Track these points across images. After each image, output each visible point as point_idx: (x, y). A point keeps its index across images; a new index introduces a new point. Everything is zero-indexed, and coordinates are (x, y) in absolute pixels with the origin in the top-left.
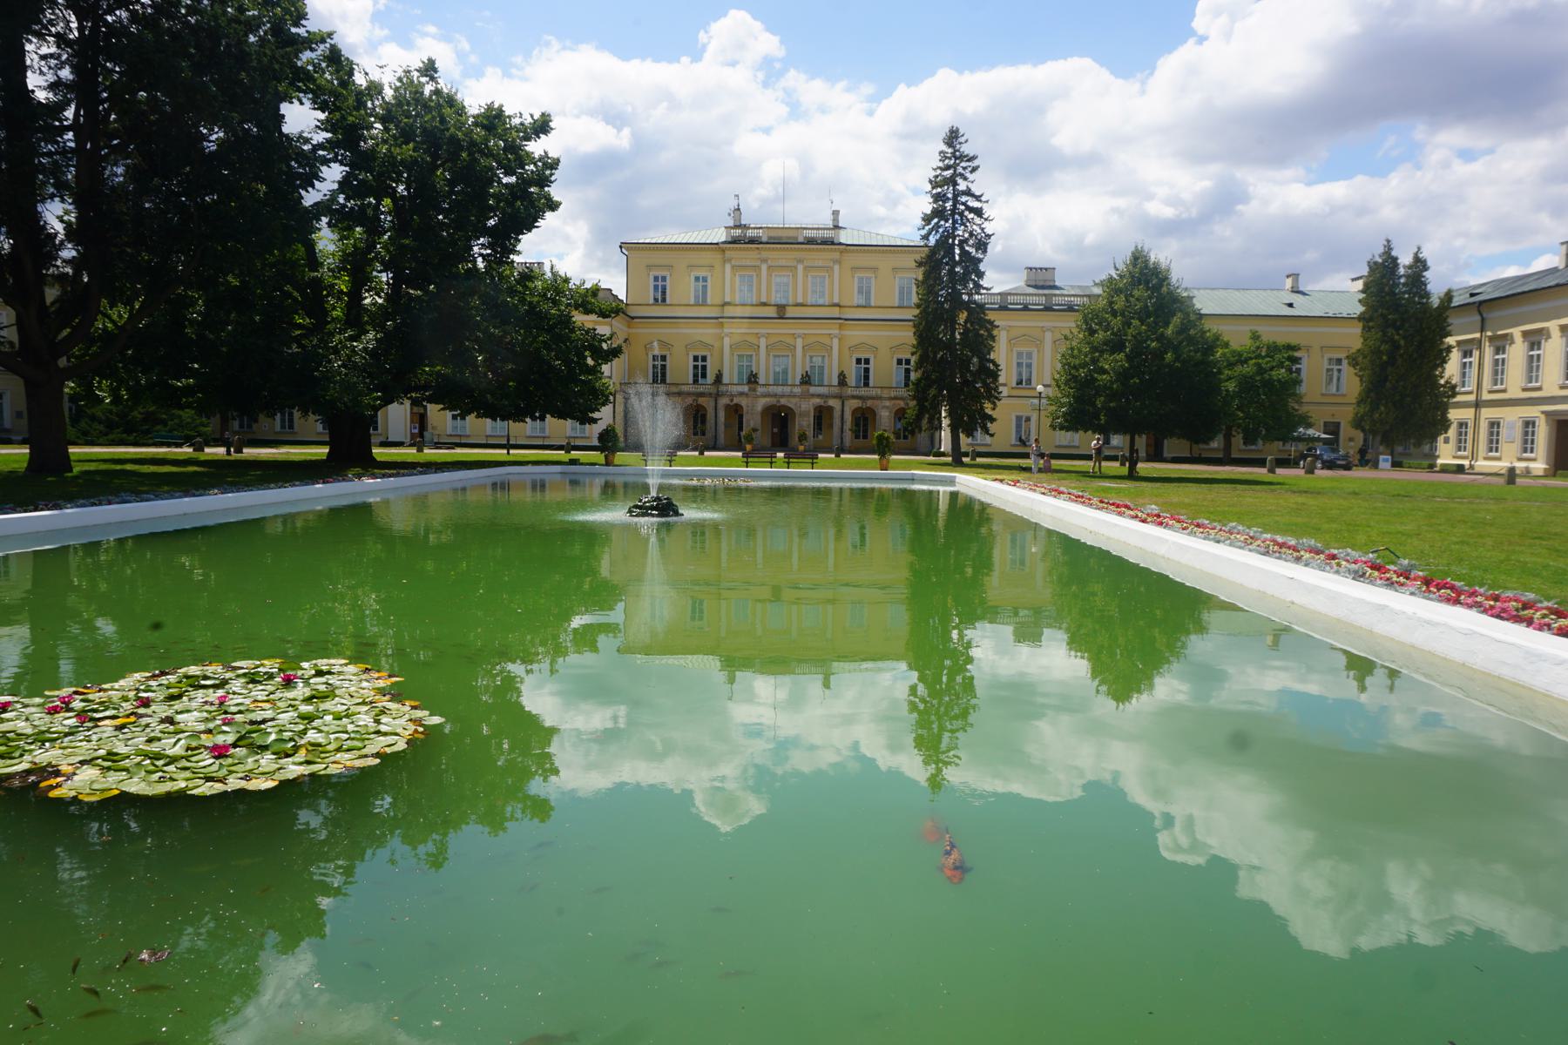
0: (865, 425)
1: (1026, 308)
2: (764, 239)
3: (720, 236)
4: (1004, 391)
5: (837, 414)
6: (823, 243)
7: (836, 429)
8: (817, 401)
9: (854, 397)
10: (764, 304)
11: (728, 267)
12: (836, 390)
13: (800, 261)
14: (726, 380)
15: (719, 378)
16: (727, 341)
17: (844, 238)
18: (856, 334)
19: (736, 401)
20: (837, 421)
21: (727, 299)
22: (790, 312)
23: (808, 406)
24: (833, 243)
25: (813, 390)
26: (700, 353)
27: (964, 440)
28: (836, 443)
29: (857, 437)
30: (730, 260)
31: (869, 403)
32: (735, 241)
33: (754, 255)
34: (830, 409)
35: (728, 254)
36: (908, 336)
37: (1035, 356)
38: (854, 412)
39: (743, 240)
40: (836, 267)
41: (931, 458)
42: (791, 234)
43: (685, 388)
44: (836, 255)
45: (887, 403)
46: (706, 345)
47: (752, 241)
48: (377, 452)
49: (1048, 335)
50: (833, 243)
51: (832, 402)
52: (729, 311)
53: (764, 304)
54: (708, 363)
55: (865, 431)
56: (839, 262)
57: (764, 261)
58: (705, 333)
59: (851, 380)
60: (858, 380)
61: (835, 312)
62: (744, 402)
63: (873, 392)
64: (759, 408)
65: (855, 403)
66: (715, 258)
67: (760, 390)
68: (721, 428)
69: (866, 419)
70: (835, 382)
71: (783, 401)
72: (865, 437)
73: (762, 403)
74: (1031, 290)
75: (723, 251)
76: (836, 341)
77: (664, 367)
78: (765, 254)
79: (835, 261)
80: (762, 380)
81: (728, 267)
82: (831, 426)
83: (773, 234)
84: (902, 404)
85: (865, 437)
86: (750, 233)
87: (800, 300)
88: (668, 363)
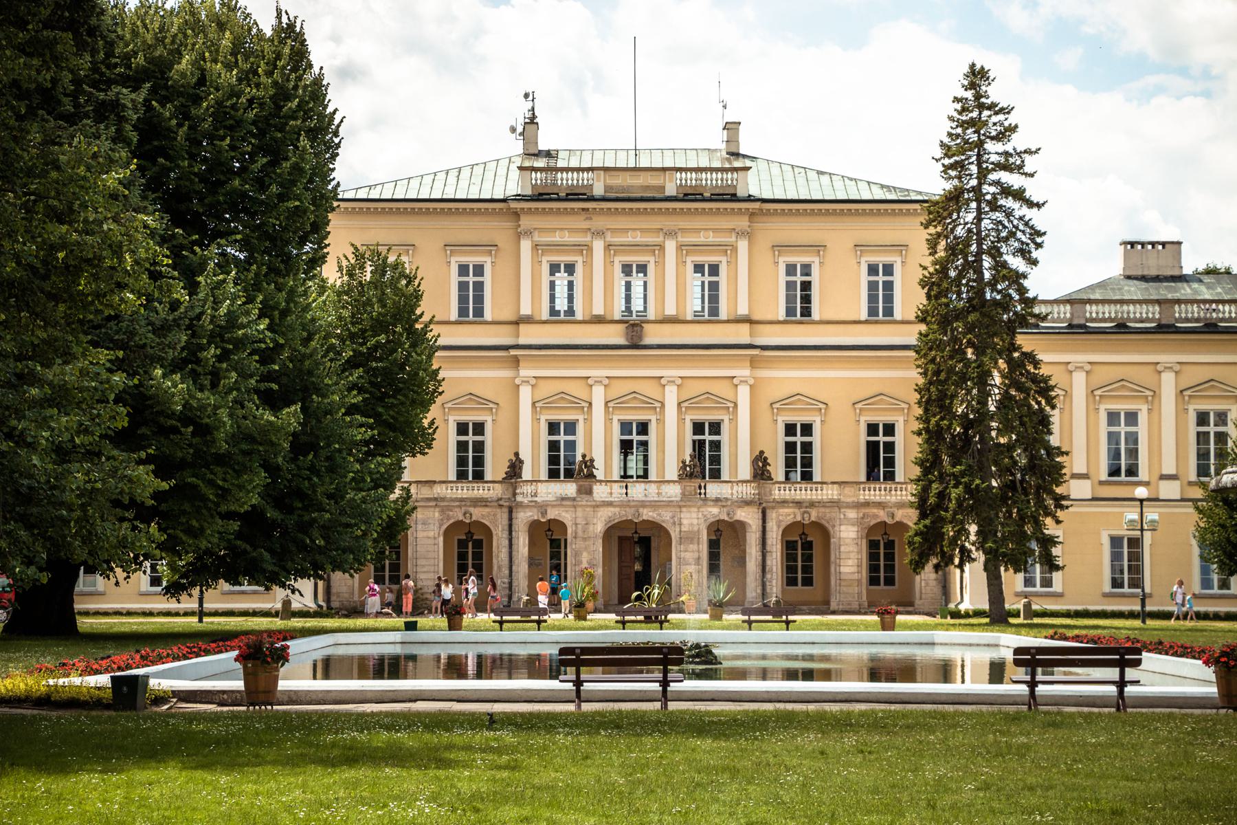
1: (1211, 328)
2: (598, 190)
3: (511, 184)
4: (1077, 489)
5: (753, 538)
6: (712, 197)
7: (752, 565)
9: (784, 503)
10: (599, 320)
11: (526, 245)
12: (749, 491)
13: (671, 234)
14: (527, 474)
15: (515, 469)
16: (526, 394)
17: (755, 184)
18: (788, 378)
19: (552, 514)
20: (753, 552)
21: (526, 310)
22: (653, 335)
24: (734, 198)
25: (713, 489)
26: (471, 418)
27: (1013, 581)
29: (791, 581)
30: (528, 233)
31: (814, 515)
32: (540, 196)
34: (738, 529)
36: (907, 377)
37: (1143, 418)
38: (787, 530)
39: (556, 194)
40: (743, 245)
41: (938, 620)
43: (439, 490)
44: (743, 223)
45: (852, 514)
47: (575, 195)
48: (84, 624)
49: (1168, 379)
50: (734, 198)
51: (742, 515)
52: (529, 335)
53: (599, 320)
54: (488, 438)
55: (807, 569)
56: (748, 235)
57: (600, 234)
59: (778, 470)
60: (790, 464)
61: (741, 334)
62: (566, 516)
63: (830, 493)
64: (599, 527)
65: (788, 515)
67: (600, 492)
68: (522, 568)
69: (808, 546)
70: (745, 471)
71: (647, 514)
72: (808, 582)
74: (1134, 290)
75: (516, 215)
76: (743, 394)
77: (479, 447)
78: (599, 222)
79: (741, 234)
80: (599, 474)
81: (526, 245)
82: (742, 561)
83: (618, 181)
84: (882, 515)
85: (808, 582)
86: (565, 180)
87: (670, 310)
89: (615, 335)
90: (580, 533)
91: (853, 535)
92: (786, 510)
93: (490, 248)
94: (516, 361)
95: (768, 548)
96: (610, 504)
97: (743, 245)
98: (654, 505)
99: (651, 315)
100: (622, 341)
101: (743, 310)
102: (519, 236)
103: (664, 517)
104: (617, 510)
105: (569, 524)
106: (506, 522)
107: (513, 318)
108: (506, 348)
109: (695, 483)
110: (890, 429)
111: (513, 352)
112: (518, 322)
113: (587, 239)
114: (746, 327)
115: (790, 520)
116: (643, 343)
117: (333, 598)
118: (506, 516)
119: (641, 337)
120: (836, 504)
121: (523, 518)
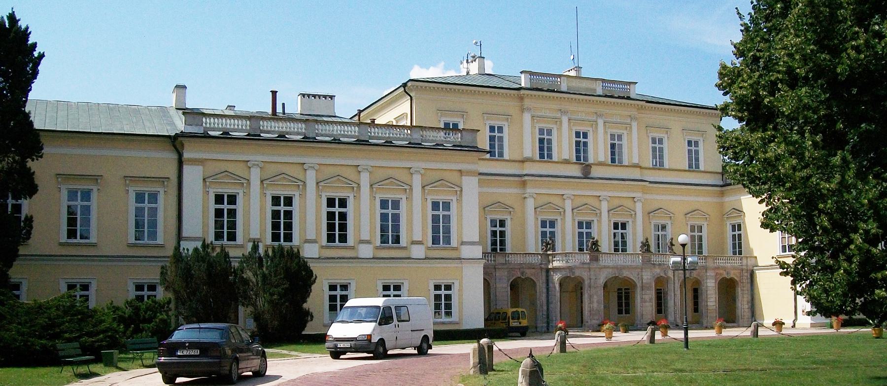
10: (567, 162)
16: (530, 204)
22: (596, 172)
23: (648, 276)
30: (529, 109)
33: (554, 106)
35: (527, 103)
46: (507, 208)
52: (529, 169)
61: (636, 174)
62: (585, 275)
64: (602, 281)
66: (509, 105)
75: (521, 98)
76: (639, 207)
81: (527, 117)
90: (592, 284)
93: (508, 116)
94: (524, 184)
96: (608, 267)
99: (591, 160)
100: (580, 175)
102: (522, 110)
103: (633, 276)
105: (586, 278)
106: (544, 278)
107: (520, 158)
110: (700, 229)
112: (523, 161)
113: (559, 115)
116: (591, 176)
118: (544, 274)
119: (590, 173)
121: (556, 277)
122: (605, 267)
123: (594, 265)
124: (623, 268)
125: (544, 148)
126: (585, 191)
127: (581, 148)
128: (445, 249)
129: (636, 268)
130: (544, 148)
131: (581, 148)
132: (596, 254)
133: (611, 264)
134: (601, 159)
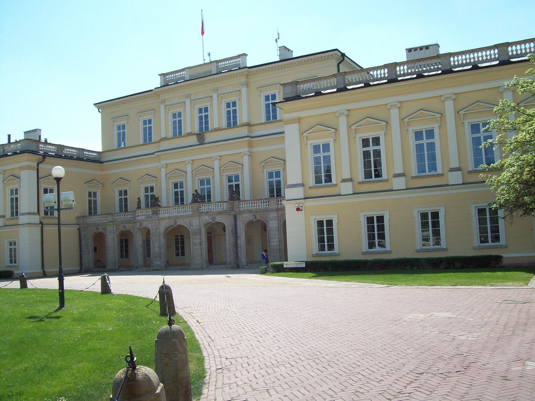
0: (127, 246)
8: (206, 219)
10: (189, 135)
16: (163, 171)
21: (163, 136)
28: (229, 257)
42: (206, 69)
53: (189, 135)
58: (149, 166)
61: (244, 131)
64: (162, 230)
71: (180, 222)
73: (164, 225)
76: (246, 161)
88: (128, 196)
89: (194, 140)
91: (276, 225)
92: (246, 215)
95: (238, 235)
97: (244, 90)
98: (181, 217)
100: (197, 143)
101: (245, 120)
104: (167, 221)
108: (153, 154)
109: (197, 205)
111: (156, 154)
114: (246, 127)
115: (248, 219)
116: (205, 142)
117: (83, 266)
120: (267, 210)
122: (164, 218)
123: (155, 216)
124: (177, 217)
125: (178, 127)
126: (202, 154)
127: (204, 121)
128: (51, 218)
129: (187, 216)
130: (178, 127)
131: (204, 121)
132: (155, 209)
133: (167, 215)
134: (216, 126)
